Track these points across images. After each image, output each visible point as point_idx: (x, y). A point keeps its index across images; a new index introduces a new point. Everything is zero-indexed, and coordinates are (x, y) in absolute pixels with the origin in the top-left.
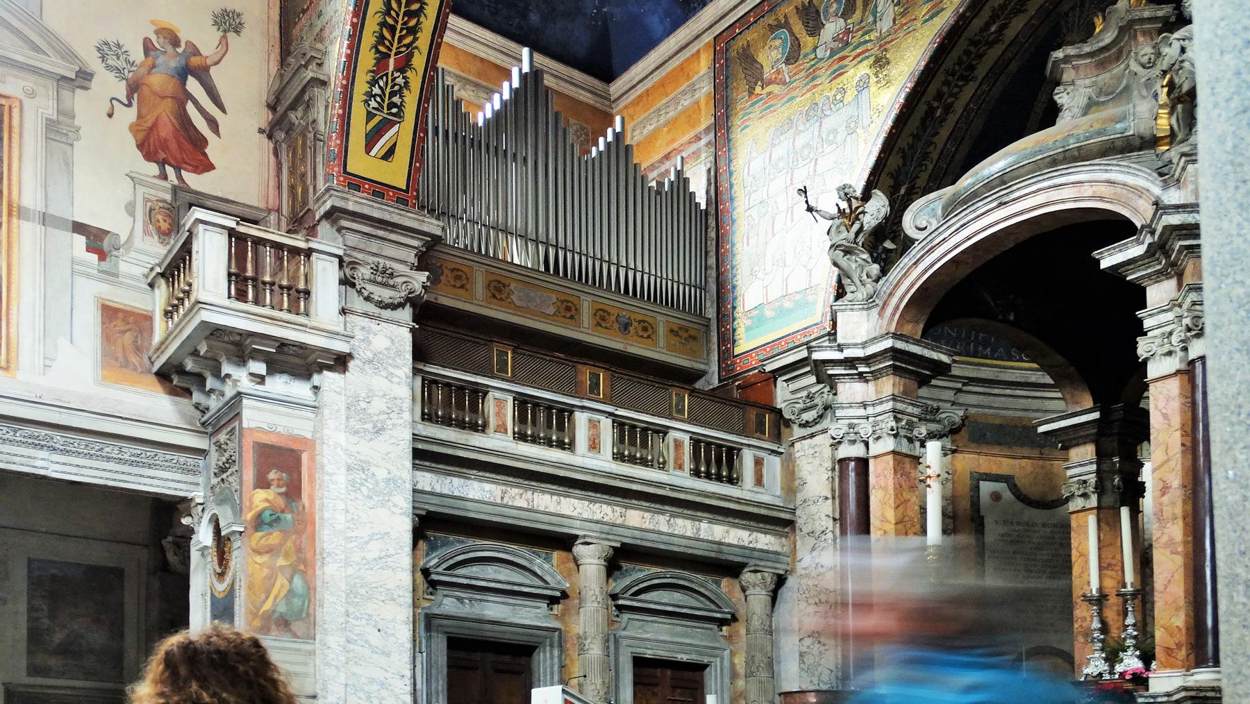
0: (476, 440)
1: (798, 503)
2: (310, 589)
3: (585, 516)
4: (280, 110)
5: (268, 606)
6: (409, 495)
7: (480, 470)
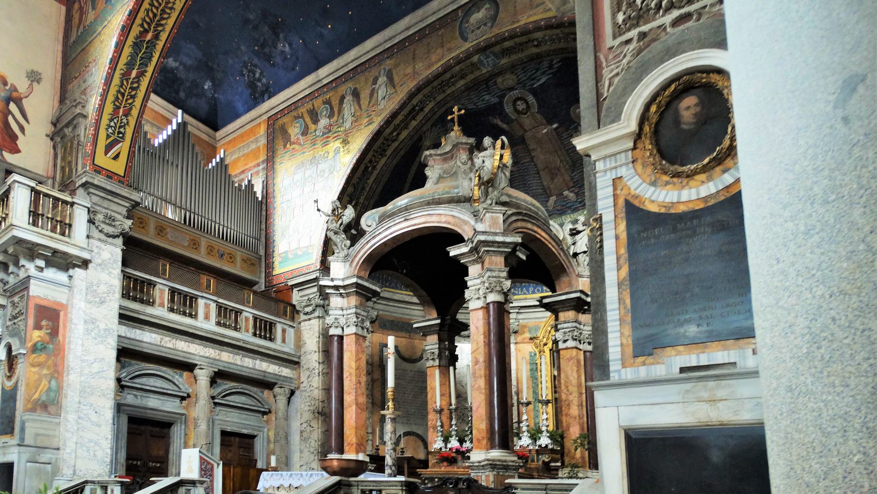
0: (149, 310)
1: (302, 353)
2: (60, 388)
3: (201, 354)
4: (59, 126)
5: (36, 396)
6: (116, 338)
7: (150, 326)
